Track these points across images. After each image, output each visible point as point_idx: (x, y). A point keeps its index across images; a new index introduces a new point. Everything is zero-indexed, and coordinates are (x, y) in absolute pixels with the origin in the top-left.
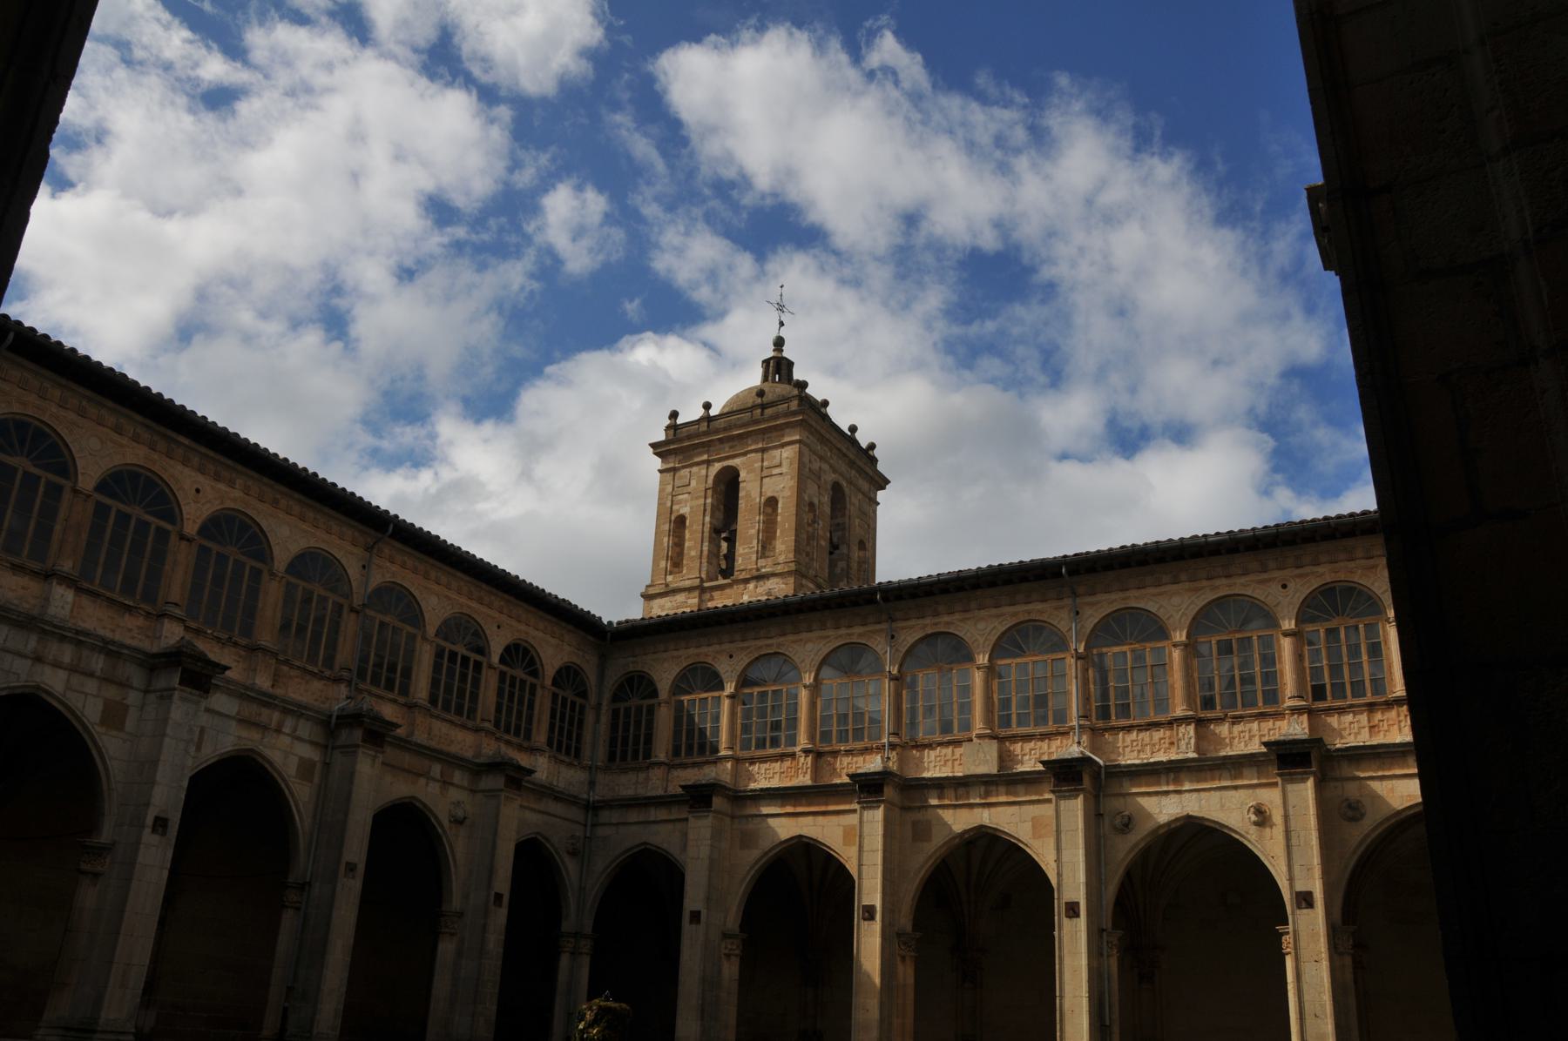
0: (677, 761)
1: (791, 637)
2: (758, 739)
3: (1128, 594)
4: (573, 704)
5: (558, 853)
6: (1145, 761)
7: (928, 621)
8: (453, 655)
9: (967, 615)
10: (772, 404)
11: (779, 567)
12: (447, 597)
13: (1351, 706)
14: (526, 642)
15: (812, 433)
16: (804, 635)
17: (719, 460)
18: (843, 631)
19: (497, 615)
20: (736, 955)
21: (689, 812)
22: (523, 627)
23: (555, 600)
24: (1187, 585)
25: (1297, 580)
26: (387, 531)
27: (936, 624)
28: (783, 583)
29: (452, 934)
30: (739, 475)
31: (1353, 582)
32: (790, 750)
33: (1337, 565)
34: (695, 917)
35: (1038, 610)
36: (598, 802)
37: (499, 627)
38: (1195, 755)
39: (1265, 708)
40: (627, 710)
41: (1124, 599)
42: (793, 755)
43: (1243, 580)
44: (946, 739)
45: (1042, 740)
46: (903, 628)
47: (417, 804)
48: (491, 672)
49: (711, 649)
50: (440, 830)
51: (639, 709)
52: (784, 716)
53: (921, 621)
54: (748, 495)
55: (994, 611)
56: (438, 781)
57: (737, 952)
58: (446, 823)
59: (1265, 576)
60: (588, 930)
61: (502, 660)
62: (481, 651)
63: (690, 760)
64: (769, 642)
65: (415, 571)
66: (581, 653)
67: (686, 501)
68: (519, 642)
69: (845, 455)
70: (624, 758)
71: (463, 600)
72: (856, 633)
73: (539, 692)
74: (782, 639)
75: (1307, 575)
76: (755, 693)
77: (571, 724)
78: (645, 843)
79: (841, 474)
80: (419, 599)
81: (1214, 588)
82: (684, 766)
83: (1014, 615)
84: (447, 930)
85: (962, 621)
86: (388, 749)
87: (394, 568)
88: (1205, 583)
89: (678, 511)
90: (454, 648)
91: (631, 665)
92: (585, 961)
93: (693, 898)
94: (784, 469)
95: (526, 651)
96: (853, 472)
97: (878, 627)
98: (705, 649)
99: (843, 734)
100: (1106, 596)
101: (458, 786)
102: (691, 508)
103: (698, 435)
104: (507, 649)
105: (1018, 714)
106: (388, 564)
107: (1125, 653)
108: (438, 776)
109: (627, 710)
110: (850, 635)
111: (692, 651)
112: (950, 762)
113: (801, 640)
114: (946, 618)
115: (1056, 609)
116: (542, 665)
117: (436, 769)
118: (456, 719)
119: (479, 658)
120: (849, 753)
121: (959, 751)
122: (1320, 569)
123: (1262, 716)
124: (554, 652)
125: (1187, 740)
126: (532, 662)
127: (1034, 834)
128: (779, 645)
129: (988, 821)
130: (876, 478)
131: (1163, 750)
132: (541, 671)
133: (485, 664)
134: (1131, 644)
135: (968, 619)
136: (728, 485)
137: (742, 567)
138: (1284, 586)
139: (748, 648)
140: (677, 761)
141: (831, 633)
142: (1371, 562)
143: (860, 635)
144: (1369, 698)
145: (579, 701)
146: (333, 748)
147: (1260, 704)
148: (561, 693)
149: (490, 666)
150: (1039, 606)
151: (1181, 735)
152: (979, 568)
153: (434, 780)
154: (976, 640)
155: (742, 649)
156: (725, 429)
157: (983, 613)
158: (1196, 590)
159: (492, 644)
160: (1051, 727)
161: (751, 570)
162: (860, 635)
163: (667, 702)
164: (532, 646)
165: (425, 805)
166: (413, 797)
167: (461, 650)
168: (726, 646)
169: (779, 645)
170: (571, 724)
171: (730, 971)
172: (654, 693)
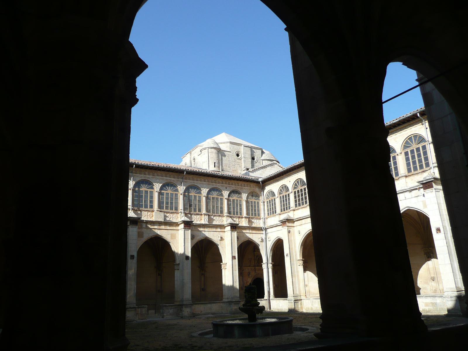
3: (194, 181)
6: (195, 223)
7: (142, 175)
9: (154, 177)
13: (236, 217)
38: (208, 223)
43: (218, 185)
44: (146, 210)
45: (171, 214)
53: (140, 175)
55: (161, 177)
59: (223, 185)
75: (230, 187)
81: (213, 185)
83: (167, 180)
85: (152, 178)
88: (211, 183)
112: (146, 216)
114: (148, 176)
122: (233, 186)
123: (220, 216)
127: (171, 238)
131: (199, 221)
135: (154, 178)
138: (226, 188)
142: (242, 187)
144: (239, 216)
147: (219, 213)
150: (173, 179)
151: (205, 218)
157: (158, 177)
158: (209, 184)
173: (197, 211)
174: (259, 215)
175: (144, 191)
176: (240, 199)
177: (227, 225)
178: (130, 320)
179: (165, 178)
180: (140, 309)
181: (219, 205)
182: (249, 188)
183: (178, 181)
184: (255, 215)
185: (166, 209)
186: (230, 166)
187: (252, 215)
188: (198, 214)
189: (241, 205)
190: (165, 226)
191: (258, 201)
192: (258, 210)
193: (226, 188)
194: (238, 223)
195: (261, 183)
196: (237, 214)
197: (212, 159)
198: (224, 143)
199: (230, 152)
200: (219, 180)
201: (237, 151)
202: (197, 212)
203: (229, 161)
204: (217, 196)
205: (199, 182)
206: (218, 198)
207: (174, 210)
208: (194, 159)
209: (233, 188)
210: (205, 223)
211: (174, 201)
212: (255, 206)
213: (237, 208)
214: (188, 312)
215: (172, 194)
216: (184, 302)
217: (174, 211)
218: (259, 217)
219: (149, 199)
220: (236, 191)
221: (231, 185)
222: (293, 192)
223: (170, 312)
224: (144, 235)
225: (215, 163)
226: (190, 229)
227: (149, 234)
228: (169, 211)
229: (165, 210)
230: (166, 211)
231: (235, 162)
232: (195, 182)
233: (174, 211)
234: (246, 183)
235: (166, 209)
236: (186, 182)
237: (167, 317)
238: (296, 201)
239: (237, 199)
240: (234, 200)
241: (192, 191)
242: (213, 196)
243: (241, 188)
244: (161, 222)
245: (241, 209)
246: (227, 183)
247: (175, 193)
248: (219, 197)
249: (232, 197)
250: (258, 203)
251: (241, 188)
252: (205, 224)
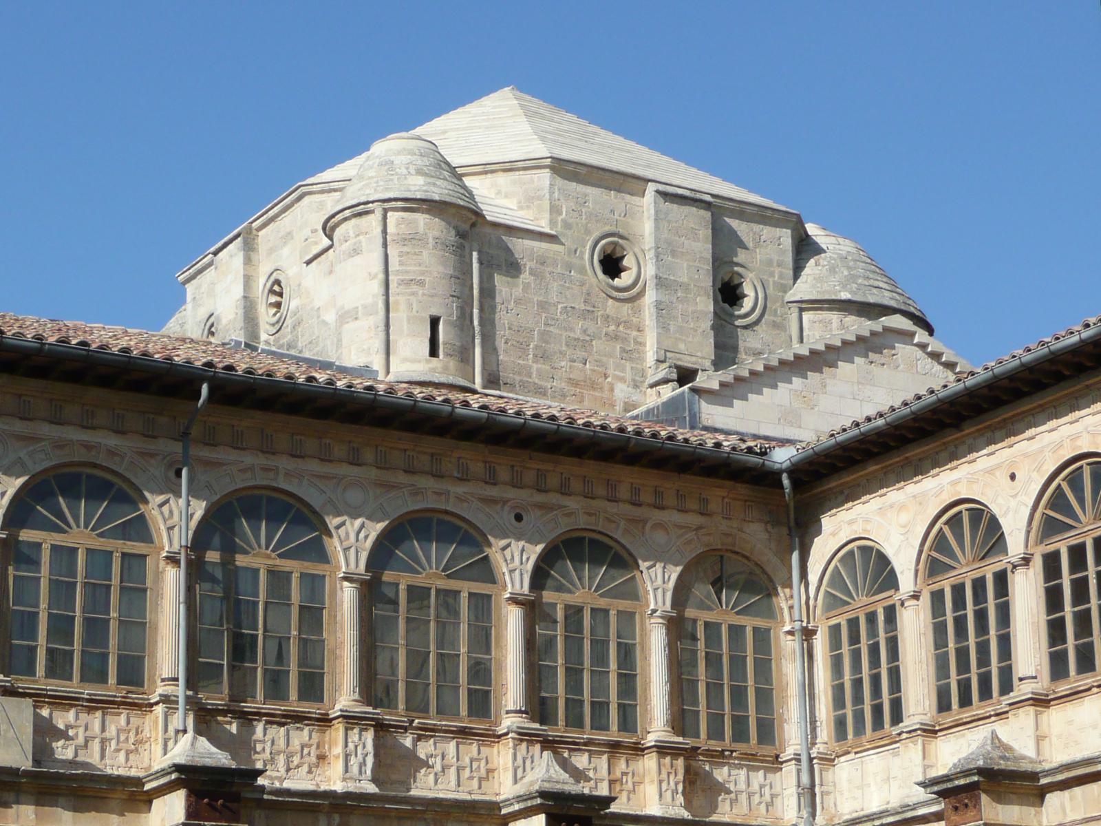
6: (277, 785)
13: (589, 743)
24: (374, 473)
25: (539, 513)
31: (611, 537)
33: (591, 502)
38: (372, 788)
39: (470, 722)
41: (266, 469)
43: (460, 489)
45: (90, 710)
55: (19, 426)
59: (492, 492)
81: (417, 492)
83: (60, 445)
88: (402, 478)
100: (231, 455)
105: (50, 652)
107: (257, 570)
115: (142, 454)
122: (572, 503)
123: (463, 733)
125: (360, 757)
131: (305, 768)
134: (269, 557)
138: (519, 518)
142: (637, 512)
144: (614, 734)
147: (464, 711)
150: (112, 441)
151: (351, 746)
158: (388, 486)
173: (293, 694)
174: (768, 731)
176: (624, 605)
177: (517, 807)
179: (46, 429)
181: (463, 650)
182: (694, 519)
183: (152, 455)
184: (740, 734)
185: (51, 672)
186: (553, 347)
187: (716, 732)
188: (298, 718)
189: (627, 654)
190: (38, 803)
191: (760, 623)
192: (765, 698)
193: (519, 518)
194: (603, 791)
195: (786, 482)
196: (600, 724)
197: (415, 288)
198: (509, 167)
199: (552, 238)
200: (471, 456)
201: (607, 229)
202: (293, 703)
203: (543, 306)
204: (449, 576)
205: (314, 466)
206: (456, 593)
207: (112, 680)
208: (276, 289)
209: (569, 515)
210: (352, 787)
211: (114, 614)
212: (738, 663)
213: (600, 676)
215: (99, 559)
217: (112, 688)
218: (767, 750)
220: (592, 541)
221: (554, 498)
222: (1038, 562)
225: (434, 322)
228: (74, 686)
229: (41, 680)
230: (55, 686)
231: (587, 314)
232: (284, 463)
233: (112, 688)
234: (671, 484)
235: (51, 672)
236: (208, 463)
238: (1056, 631)
239: (603, 603)
240: (574, 613)
241: (257, 537)
242: (420, 580)
243: (634, 521)
244: (13, 772)
245: (628, 683)
246: (529, 477)
247: (119, 546)
248: (466, 588)
249: (560, 588)
250: (763, 639)
251: (634, 521)
252: (348, 795)
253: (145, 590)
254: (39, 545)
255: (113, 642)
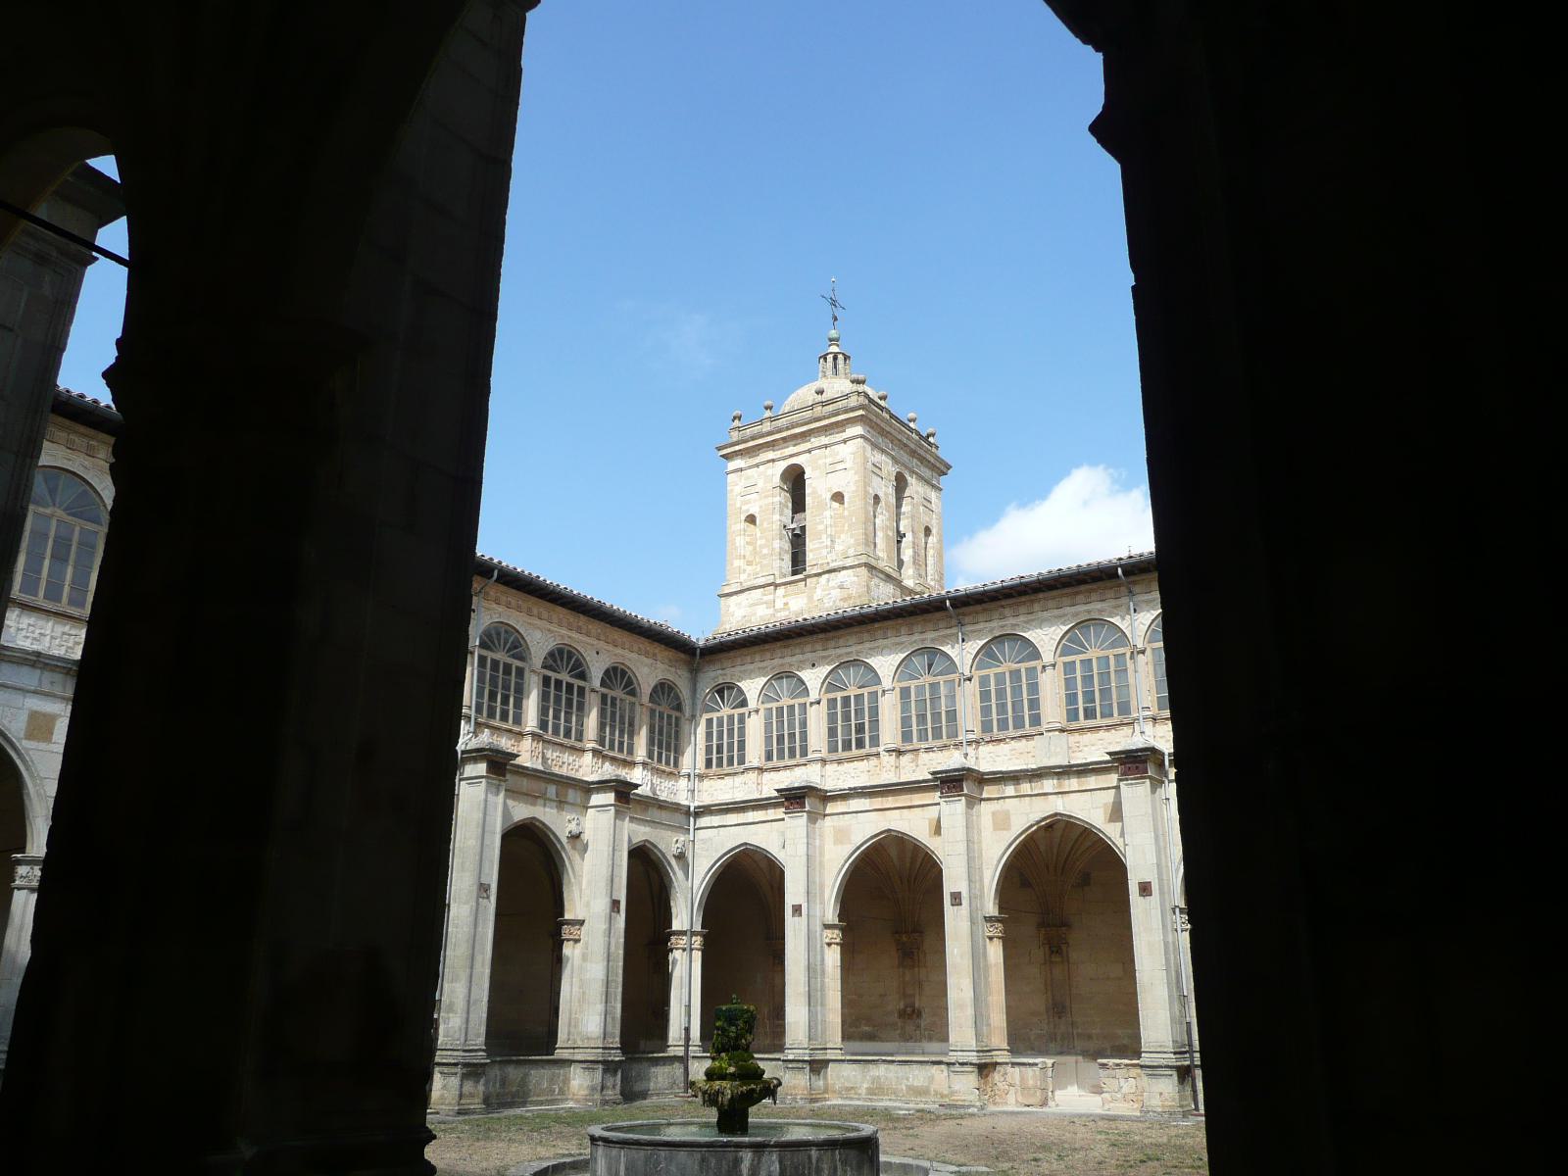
0: (770, 765)
1: (867, 645)
2: (844, 741)
4: (669, 717)
5: (665, 858)
7: (994, 624)
8: (558, 683)
9: (1030, 617)
10: (833, 401)
11: (849, 560)
12: (549, 630)
14: (623, 664)
15: (872, 428)
16: (881, 642)
17: (784, 458)
18: (916, 637)
19: (596, 642)
20: (837, 944)
21: (786, 813)
22: (619, 651)
23: (647, 625)
26: (492, 576)
27: (1002, 627)
28: (854, 576)
29: (577, 941)
30: (804, 473)
32: (874, 750)
34: (797, 910)
35: (1095, 607)
36: (699, 807)
37: (598, 653)
40: (720, 721)
42: (878, 755)
46: (973, 632)
47: (537, 824)
48: (593, 695)
49: (794, 659)
50: (559, 847)
51: (731, 718)
52: (867, 718)
53: (988, 625)
54: (814, 492)
55: (1056, 612)
56: (554, 801)
57: (838, 940)
58: (564, 840)
60: (698, 927)
61: (603, 684)
62: (582, 676)
63: (782, 764)
64: (849, 650)
65: (519, 609)
66: (673, 669)
67: (755, 501)
68: (616, 665)
69: (906, 445)
70: (720, 764)
71: (564, 631)
72: (929, 638)
73: (638, 708)
74: (860, 647)
76: (839, 699)
77: (669, 736)
78: (746, 844)
79: (903, 465)
80: (525, 635)
82: (776, 769)
83: (1076, 615)
84: (571, 937)
86: (508, 776)
87: (500, 609)
89: (748, 510)
90: (559, 676)
91: (720, 678)
92: (697, 956)
93: (794, 893)
94: (847, 465)
95: (624, 673)
96: (915, 460)
97: (949, 631)
98: (788, 660)
99: (923, 732)
101: (572, 804)
102: (761, 507)
103: (762, 436)
104: (607, 672)
106: (495, 606)
108: (554, 797)
109: (720, 721)
110: (923, 640)
111: (777, 661)
113: (878, 647)
114: (1012, 621)
116: (639, 685)
117: (552, 790)
118: (566, 741)
119: (582, 683)
120: (928, 750)
121: (1031, 743)
124: (649, 670)
126: (630, 683)
128: (858, 652)
129: (1061, 808)
130: (938, 465)
132: (638, 690)
133: (587, 690)
135: (1033, 620)
136: (795, 482)
137: (814, 563)
139: (829, 656)
140: (770, 765)
141: (904, 639)
143: (933, 640)
145: (674, 714)
146: (460, 780)
148: (658, 709)
149: (593, 690)
150: (1099, 606)
152: (1040, 574)
153: (551, 800)
154: (1042, 639)
155: (823, 657)
156: (788, 429)
159: (592, 669)
160: (1116, 718)
161: (822, 564)
162: (933, 640)
163: (757, 711)
164: (629, 668)
165: (544, 824)
166: (534, 818)
167: (565, 677)
168: (809, 655)
169: (858, 652)
170: (669, 736)
171: (833, 957)
172: (744, 703)
175: (1007, 675)
178: (960, 1103)
180: (1017, 1069)
185: (1086, 717)
190: (1078, 778)
207: (1116, 714)
214: (1161, 1094)
215: (1015, 675)
216: (829, 1051)
219: (1025, 695)
223: (1124, 1090)
224: (1013, 818)
226: (1144, 778)
227: (1027, 814)
228: (1098, 721)
230: (1091, 723)
233: (1116, 718)
235: (1086, 717)
237: (1112, 1104)
253: (1126, 670)
254: (1074, 662)
255: (1114, 697)
